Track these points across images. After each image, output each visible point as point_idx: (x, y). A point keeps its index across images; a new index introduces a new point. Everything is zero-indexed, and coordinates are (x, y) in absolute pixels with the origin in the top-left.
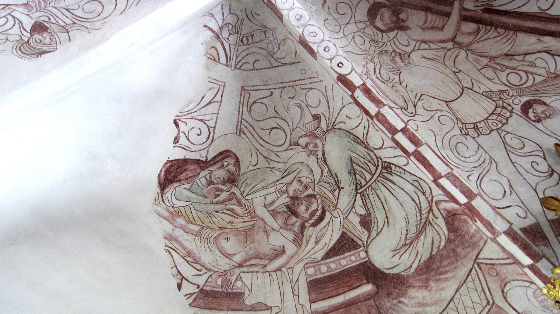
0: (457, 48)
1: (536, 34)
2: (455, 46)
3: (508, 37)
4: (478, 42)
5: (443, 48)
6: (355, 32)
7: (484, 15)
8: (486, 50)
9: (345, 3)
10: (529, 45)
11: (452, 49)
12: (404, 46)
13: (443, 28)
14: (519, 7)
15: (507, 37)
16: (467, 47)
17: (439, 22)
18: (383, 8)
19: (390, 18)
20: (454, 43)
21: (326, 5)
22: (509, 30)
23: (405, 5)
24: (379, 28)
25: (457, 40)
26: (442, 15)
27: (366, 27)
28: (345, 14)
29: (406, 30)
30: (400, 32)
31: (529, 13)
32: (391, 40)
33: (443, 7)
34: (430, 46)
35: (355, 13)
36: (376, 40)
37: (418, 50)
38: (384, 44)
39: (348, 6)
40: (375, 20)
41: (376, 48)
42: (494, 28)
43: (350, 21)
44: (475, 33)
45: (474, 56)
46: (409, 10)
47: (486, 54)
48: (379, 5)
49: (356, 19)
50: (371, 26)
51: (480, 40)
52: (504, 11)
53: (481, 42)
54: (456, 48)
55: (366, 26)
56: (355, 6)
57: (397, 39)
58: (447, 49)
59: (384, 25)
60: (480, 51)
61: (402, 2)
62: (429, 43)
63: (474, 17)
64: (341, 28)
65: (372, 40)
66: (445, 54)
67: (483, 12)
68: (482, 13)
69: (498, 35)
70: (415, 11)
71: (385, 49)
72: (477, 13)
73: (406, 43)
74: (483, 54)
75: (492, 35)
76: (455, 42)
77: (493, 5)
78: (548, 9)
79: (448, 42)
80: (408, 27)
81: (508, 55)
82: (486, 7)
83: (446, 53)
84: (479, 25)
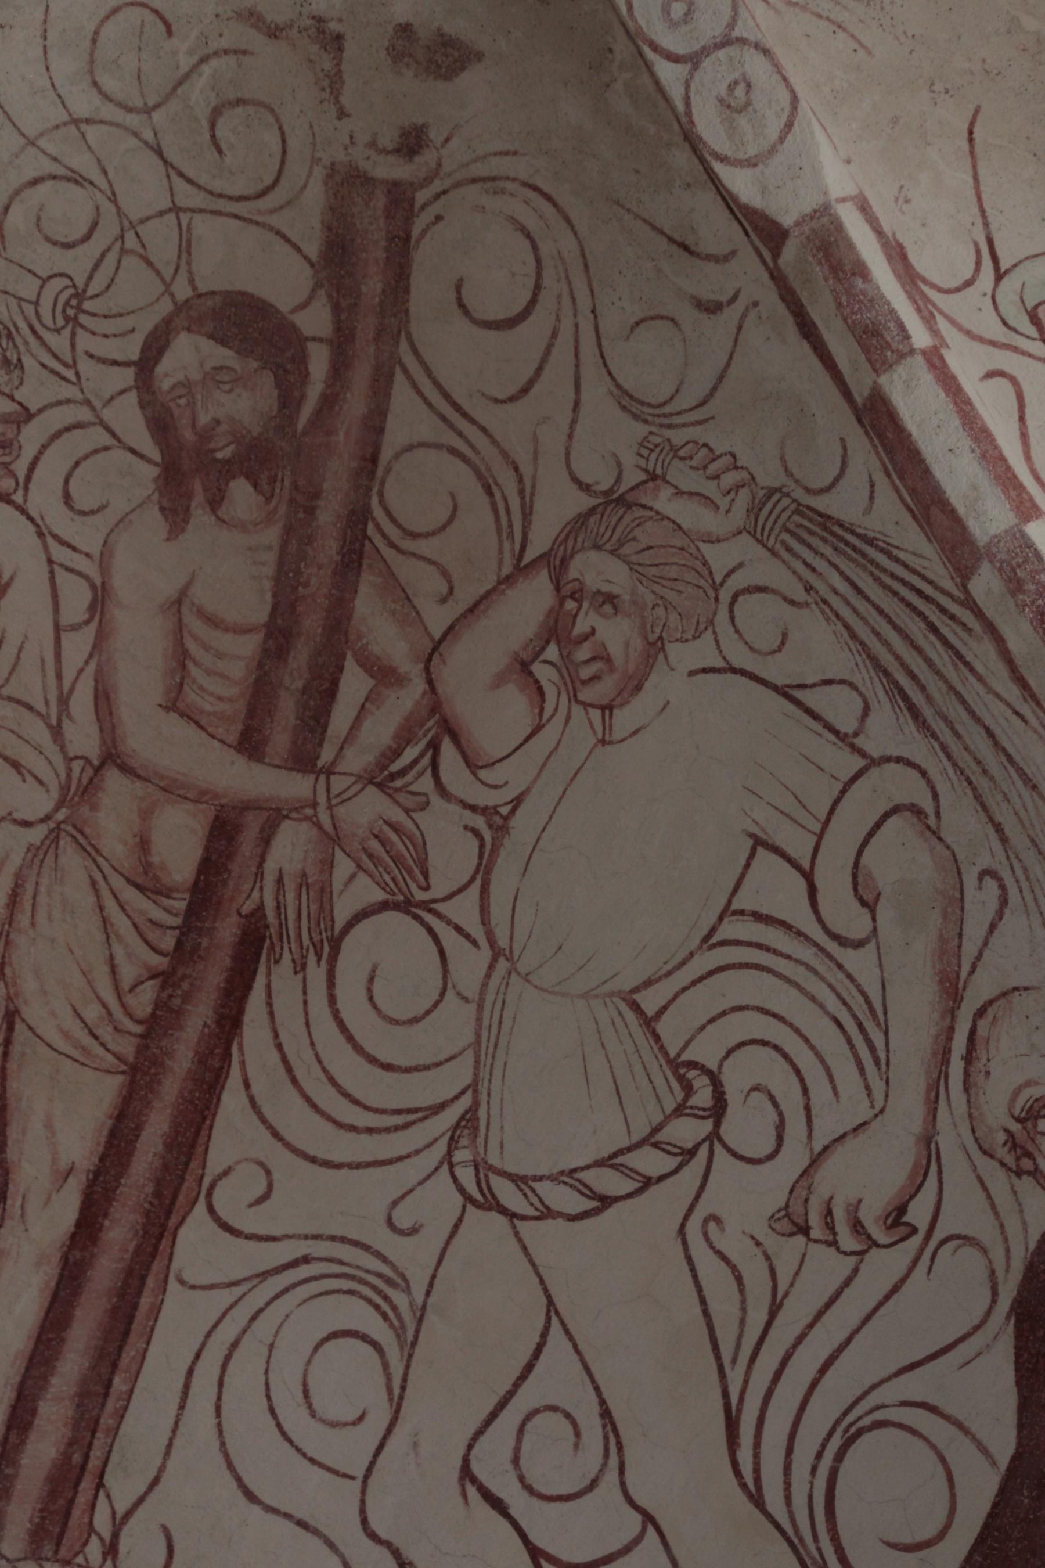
0: (69, 776)
1: (102, 1159)
2: (77, 766)
3: (106, 1032)
4: (94, 883)
5: (64, 701)
6: (113, 199)
7: (234, 919)
8: (50, 918)
9: (283, 162)
10: (49, 1125)
11: (62, 748)
12: (67, 481)
13: (182, 715)
14: (247, 1085)
15: (110, 1029)
16: (69, 828)
17: (211, 694)
18: (278, 385)
19: (224, 427)
20: (96, 762)
21: (255, 39)
22: (141, 1036)
23: (301, 515)
24: (161, 351)
25: (113, 777)
26: (251, 712)
27: (158, 273)
28: (220, 151)
29: (162, 509)
30: (154, 471)
31: (211, 1127)
32: (93, 409)
33: (293, 721)
34: (74, 628)
35: (236, 216)
36: (83, 319)
37: (50, 561)
38: (65, 365)
39: (268, 180)
40: (211, 336)
41: (30, 310)
42: (161, 968)
43: (181, 175)
44: (146, 873)
45: (16, 860)
46: (272, 535)
47: (23, 919)
48: (289, 367)
49: (198, 218)
50: (166, 307)
51: (105, 892)
52: (241, 1011)
53: (92, 899)
54: (69, 770)
55: (168, 273)
56: (274, 220)
57: (106, 449)
58: (59, 721)
59: (180, 384)
60: (43, 889)
61: (317, 495)
62: (94, 625)
63: (230, 872)
64: (130, 110)
65: (80, 296)
66: (30, 708)
67: (252, 914)
68: (245, 911)
69: (126, 985)
70: (269, 570)
71: (27, 361)
72: (247, 887)
73: (84, 500)
74: (27, 906)
75: (129, 955)
76: (102, 765)
77: (277, 962)
78: (211, 1209)
79: (101, 730)
80: (186, 521)
81: (11, 1028)
82: (272, 930)
83: (39, 714)
84: (187, 896)
